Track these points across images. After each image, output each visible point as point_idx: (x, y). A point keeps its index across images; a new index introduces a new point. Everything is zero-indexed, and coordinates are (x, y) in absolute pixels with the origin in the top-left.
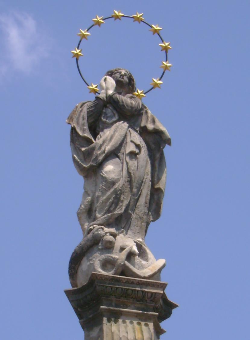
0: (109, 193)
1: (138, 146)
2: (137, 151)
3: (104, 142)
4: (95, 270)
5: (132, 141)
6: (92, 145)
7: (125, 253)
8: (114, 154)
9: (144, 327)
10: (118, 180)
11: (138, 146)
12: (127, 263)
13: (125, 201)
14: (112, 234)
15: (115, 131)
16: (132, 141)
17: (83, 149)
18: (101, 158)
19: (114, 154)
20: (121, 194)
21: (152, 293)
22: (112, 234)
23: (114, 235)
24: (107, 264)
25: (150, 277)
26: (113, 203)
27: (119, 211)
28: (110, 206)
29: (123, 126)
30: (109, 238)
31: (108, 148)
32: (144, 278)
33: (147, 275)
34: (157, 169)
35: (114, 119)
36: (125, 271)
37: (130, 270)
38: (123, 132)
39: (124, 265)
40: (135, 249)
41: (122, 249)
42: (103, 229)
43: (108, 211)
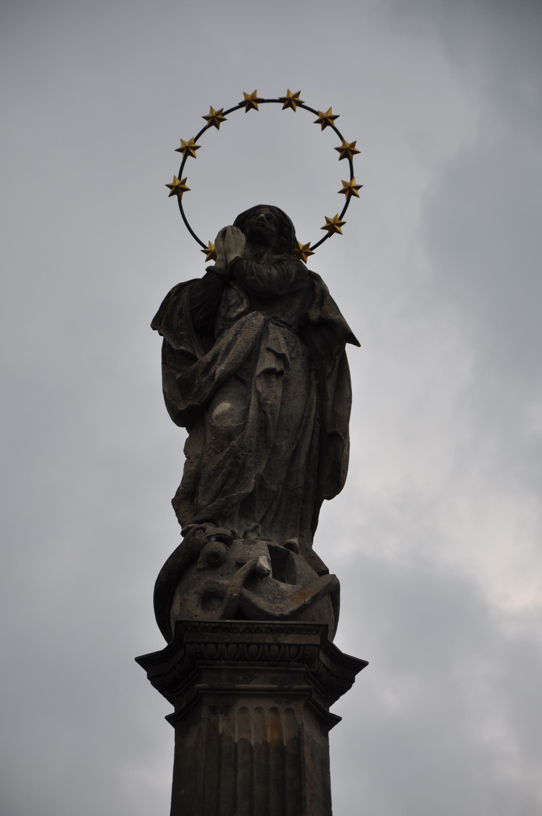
0: (220, 457)
1: (280, 357)
3: (215, 358)
5: (269, 349)
7: (242, 572)
9: (283, 717)
11: (280, 357)
12: (247, 593)
14: (221, 538)
15: (238, 333)
16: (269, 349)
18: (208, 390)
23: (227, 541)
25: (295, 614)
26: (229, 475)
31: (220, 369)
32: (283, 617)
33: (286, 612)
34: (330, 396)
35: (241, 309)
37: (253, 606)
38: (250, 333)
39: (241, 596)
40: (264, 563)
42: (204, 529)
43: (221, 492)
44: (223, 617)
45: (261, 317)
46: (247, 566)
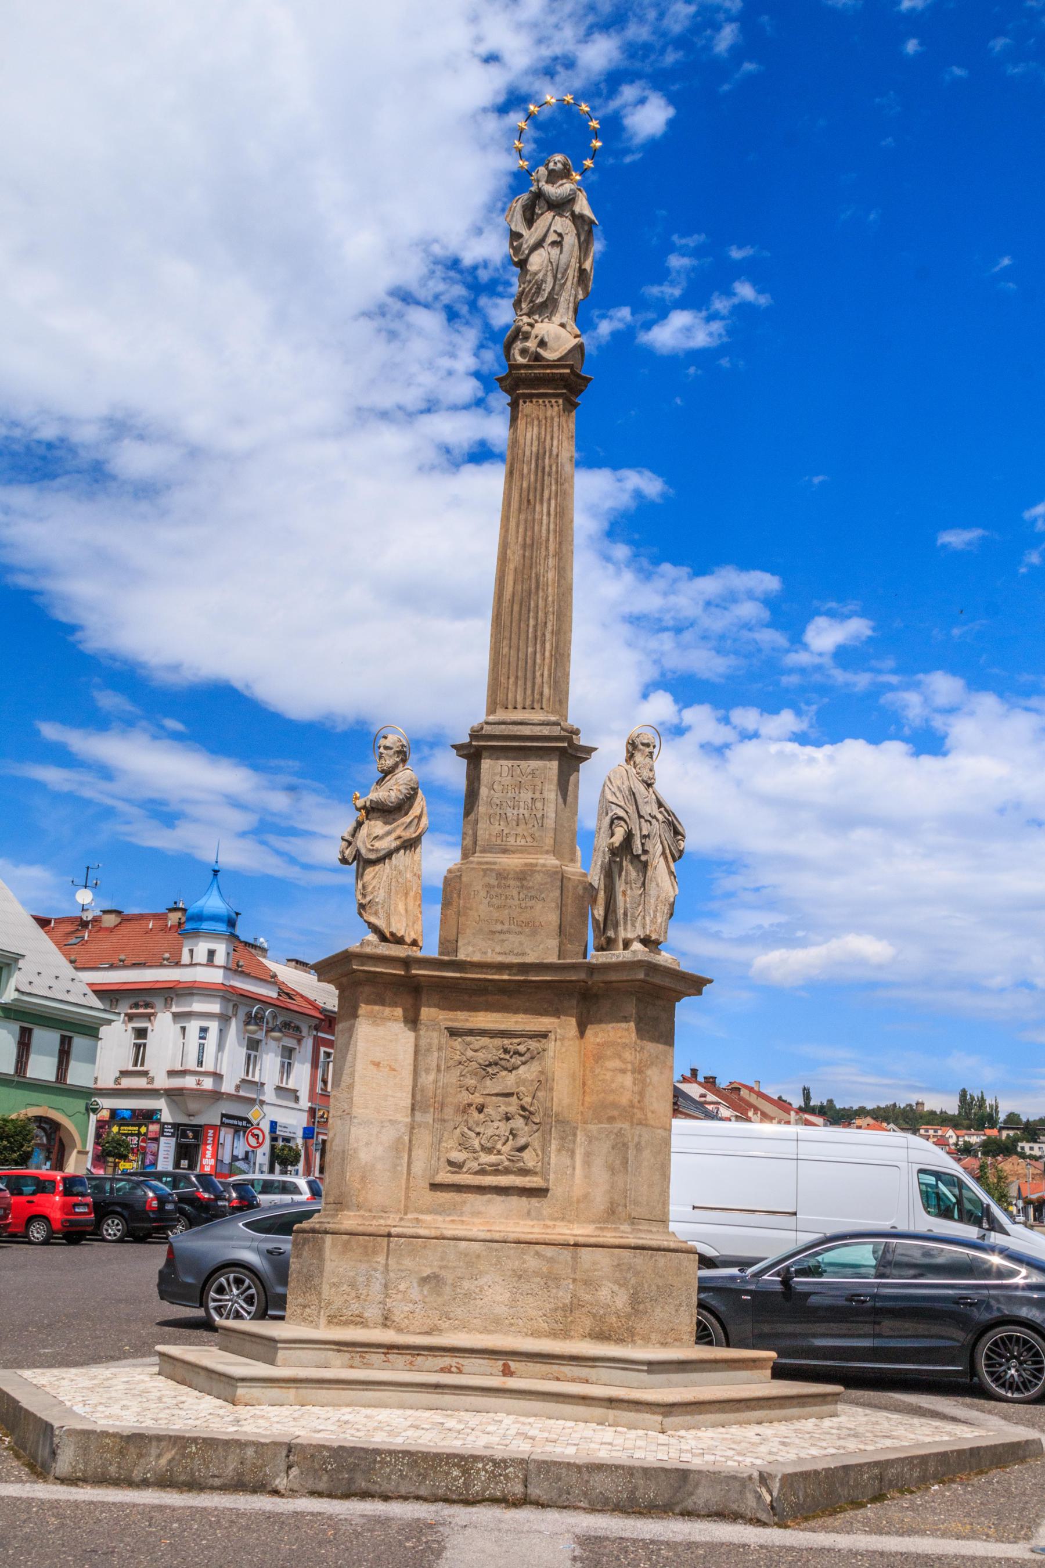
2: (559, 239)
4: (515, 360)
6: (521, 240)
8: (539, 245)
10: (540, 271)
11: (560, 235)
12: (540, 351)
13: (548, 287)
14: (530, 324)
17: (515, 244)
19: (539, 245)
20: (541, 284)
21: (561, 374)
22: (530, 324)
23: (532, 325)
24: (524, 352)
25: (559, 360)
26: (535, 292)
27: (540, 300)
28: (533, 297)
29: (549, 215)
30: (526, 328)
33: (556, 358)
36: (537, 357)
37: (541, 356)
41: (536, 337)
43: (531, 301)
44: (529, 361)
45: (552, 214)
46: (539, 338)
